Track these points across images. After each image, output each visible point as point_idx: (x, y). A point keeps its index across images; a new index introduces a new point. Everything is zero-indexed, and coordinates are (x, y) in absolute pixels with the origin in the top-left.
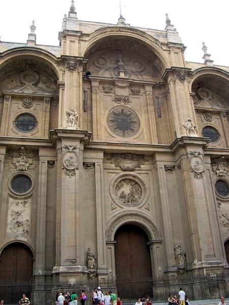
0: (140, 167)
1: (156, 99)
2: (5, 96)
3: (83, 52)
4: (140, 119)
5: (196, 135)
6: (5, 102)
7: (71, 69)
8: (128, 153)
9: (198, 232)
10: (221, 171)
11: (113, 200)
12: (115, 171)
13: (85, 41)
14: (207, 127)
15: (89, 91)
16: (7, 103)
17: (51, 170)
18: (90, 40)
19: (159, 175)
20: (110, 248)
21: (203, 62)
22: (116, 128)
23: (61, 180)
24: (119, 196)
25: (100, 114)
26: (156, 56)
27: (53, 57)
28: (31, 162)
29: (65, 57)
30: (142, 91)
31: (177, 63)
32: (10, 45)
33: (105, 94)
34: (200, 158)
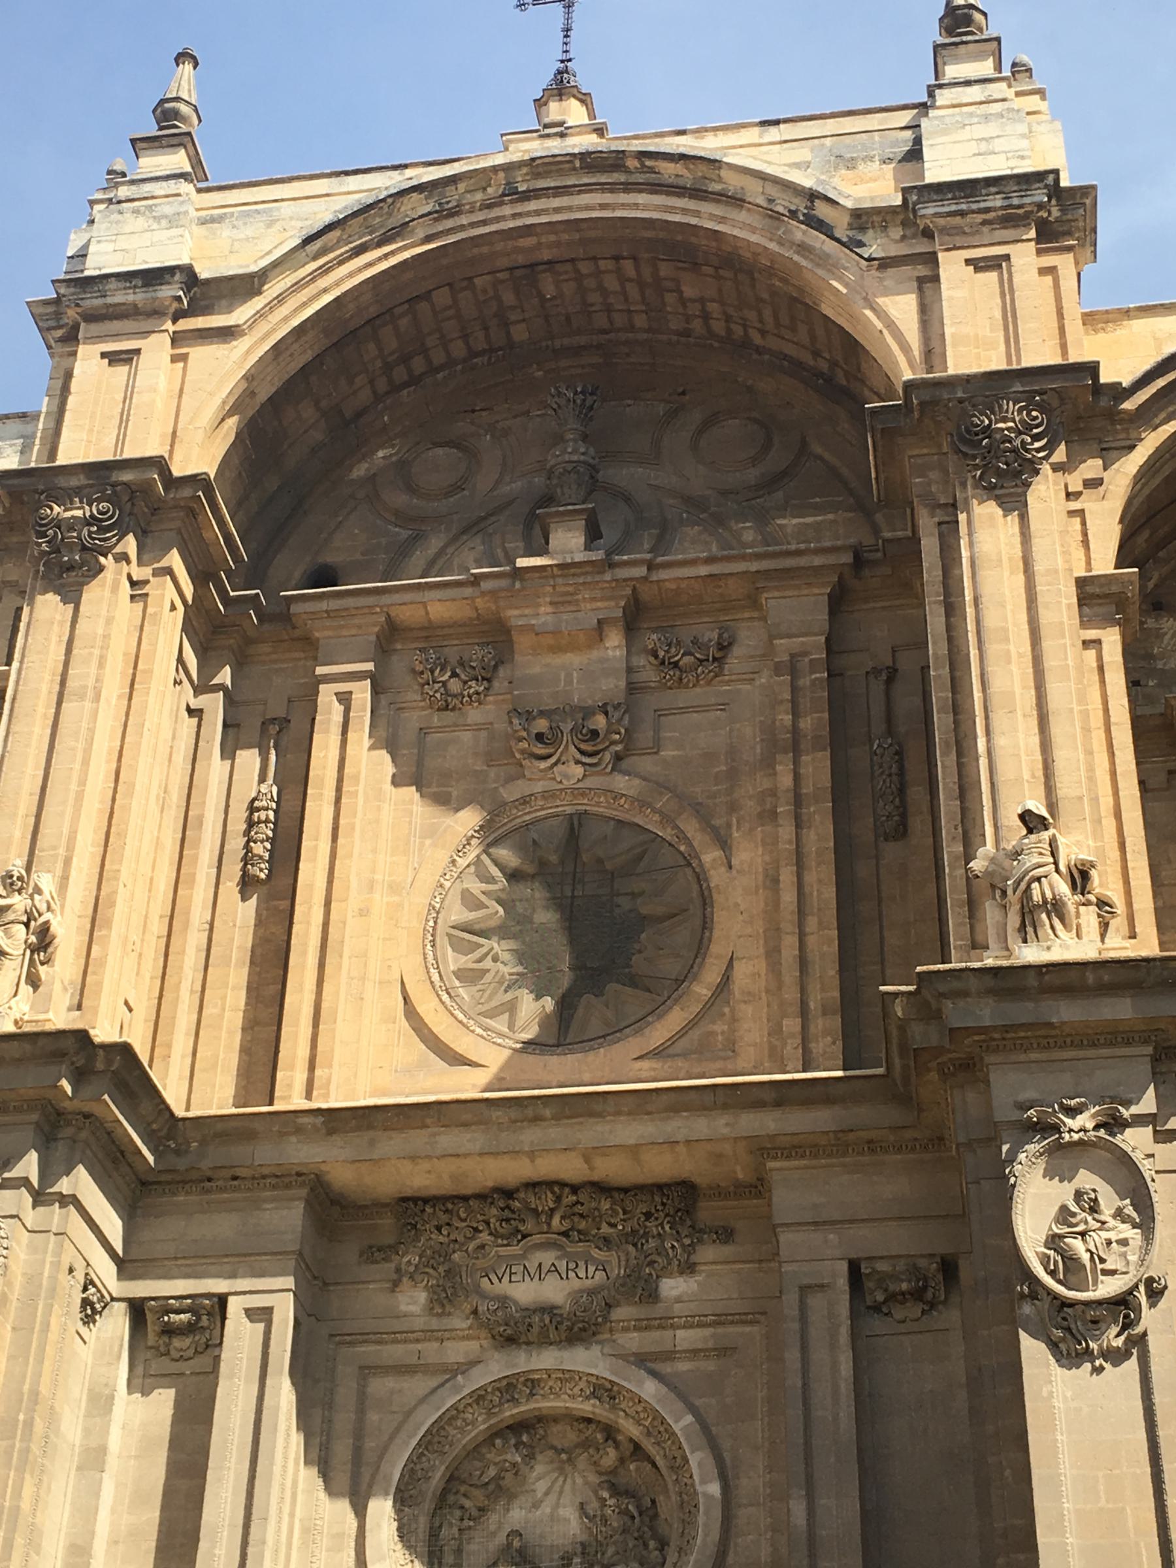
4: (717, 877)
8: (532, 1185)
13: (227, 334)
18: (260, 315)
30: (749, 639)
33: (436, 720)
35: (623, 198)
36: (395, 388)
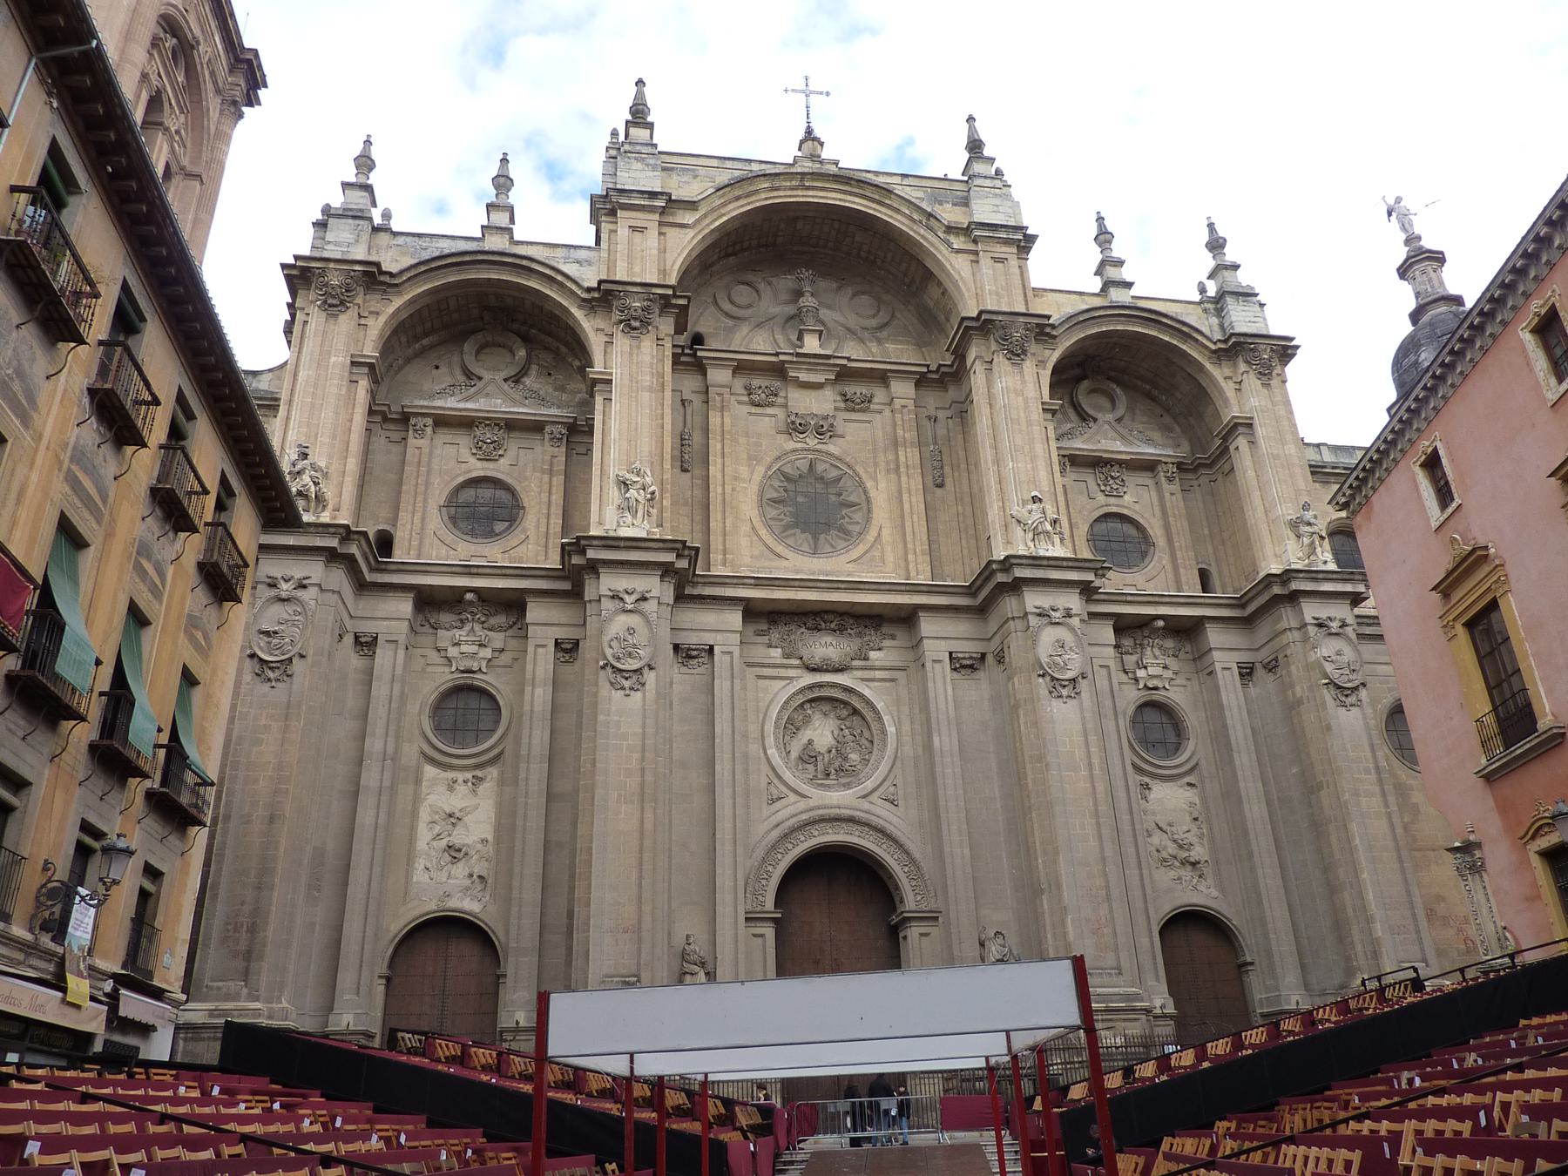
0: (866, 659)
1: (928, 425)
2: (413, 421)
3: (677, 267)
4: (872, 493)
5: (1058, 551)
6: (412, 441)
7: (635, 325)
8: (827, 612)
9: (1059, 886)
10: (1152, 671)
11: (773, 769)
12: (783, 672)
14: (1107, 516)
15: (697, 400)
16: (419, 442)
17: (567, 668)
18: (698, 221)
19: (930, 685)
20: (762, 936)
21: (1097, 290)
22: (786, 528)
23: (595, 705)
24: (794, 755)
25: (736, 478)
26: (929, 275)
27: (574, 287)
28: (498, 645)
29: (614, 287)
31: (998, 294)
32: (425, 243)
33: (754, 410)
34: (1072, 629)
35: (849, 198)
36: (728, 255)
